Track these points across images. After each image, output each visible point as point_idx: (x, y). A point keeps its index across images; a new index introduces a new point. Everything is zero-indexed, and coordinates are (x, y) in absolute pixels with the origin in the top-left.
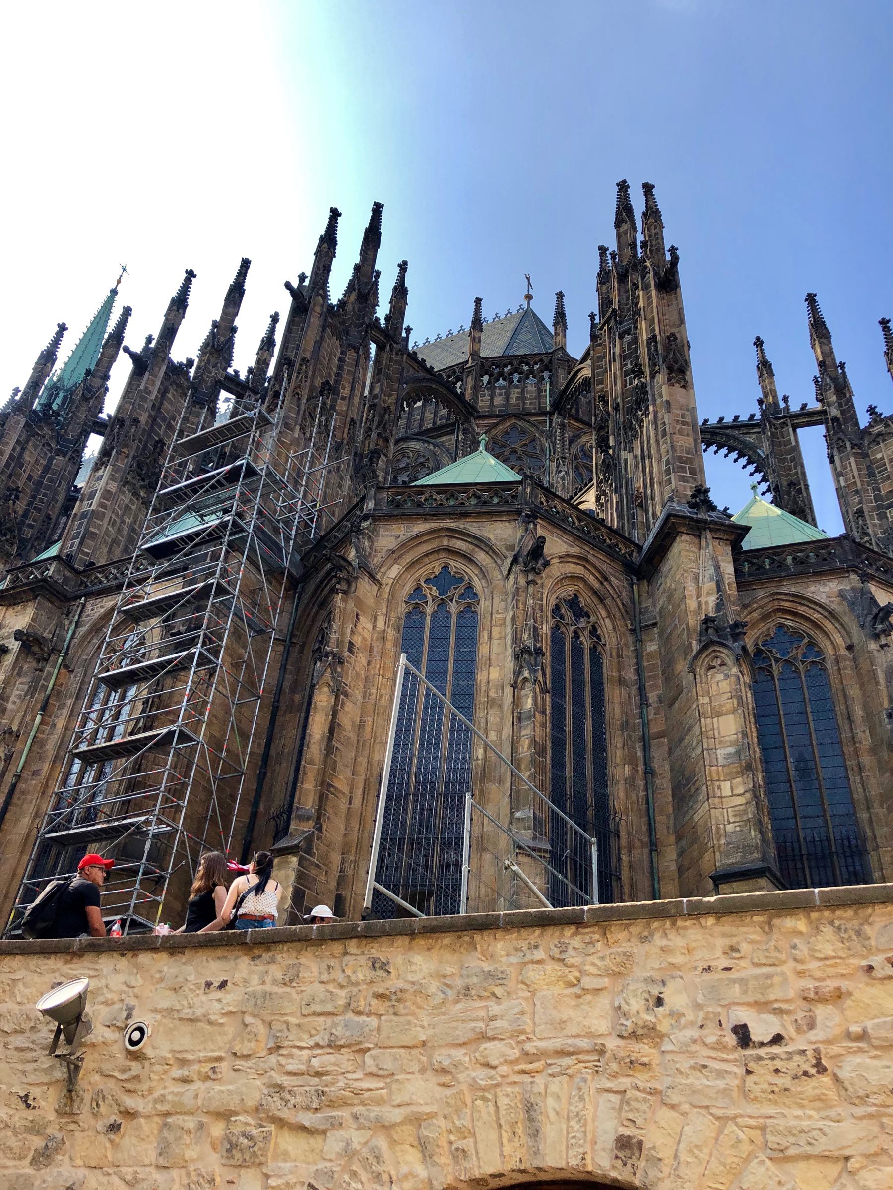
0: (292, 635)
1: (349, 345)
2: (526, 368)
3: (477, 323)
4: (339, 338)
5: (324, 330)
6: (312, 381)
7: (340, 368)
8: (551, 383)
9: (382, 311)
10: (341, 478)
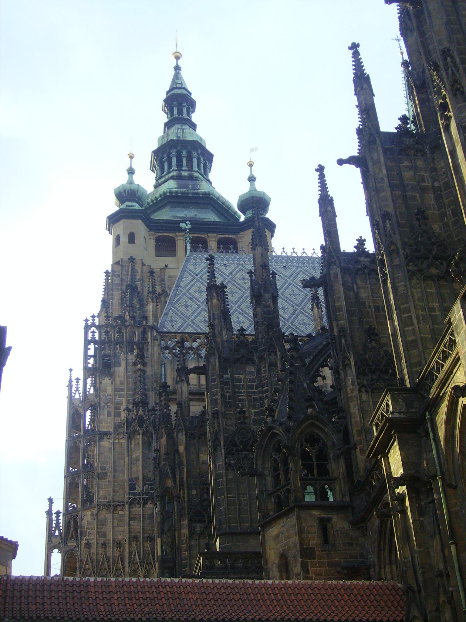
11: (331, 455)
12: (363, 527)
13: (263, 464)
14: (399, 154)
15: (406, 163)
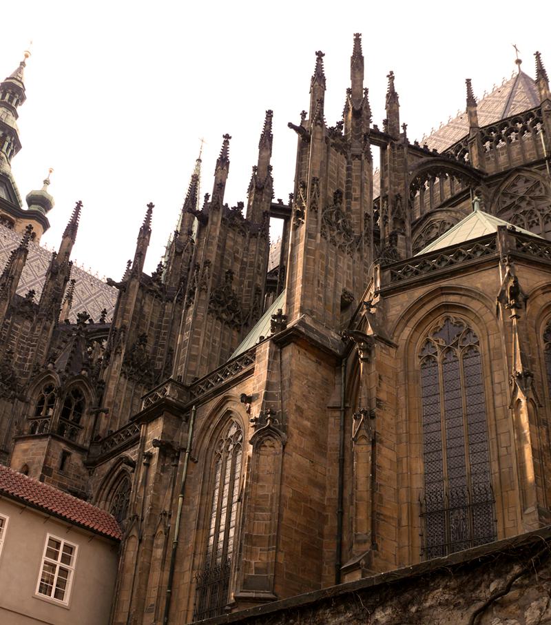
0: (345, 402)
1: (353, 155)
2: (519, 126)
3: (471, 101)
4: (344, 153)
5: (328, 151)
6: (326, 194)
7: (349, 175)
8: (544, 132)
9: (378, 117)
10: (366, 265)
11: (86, 410)
12: (91, 469)
13: (32, 395)
14: (229, 227)
15: (231, 235)
